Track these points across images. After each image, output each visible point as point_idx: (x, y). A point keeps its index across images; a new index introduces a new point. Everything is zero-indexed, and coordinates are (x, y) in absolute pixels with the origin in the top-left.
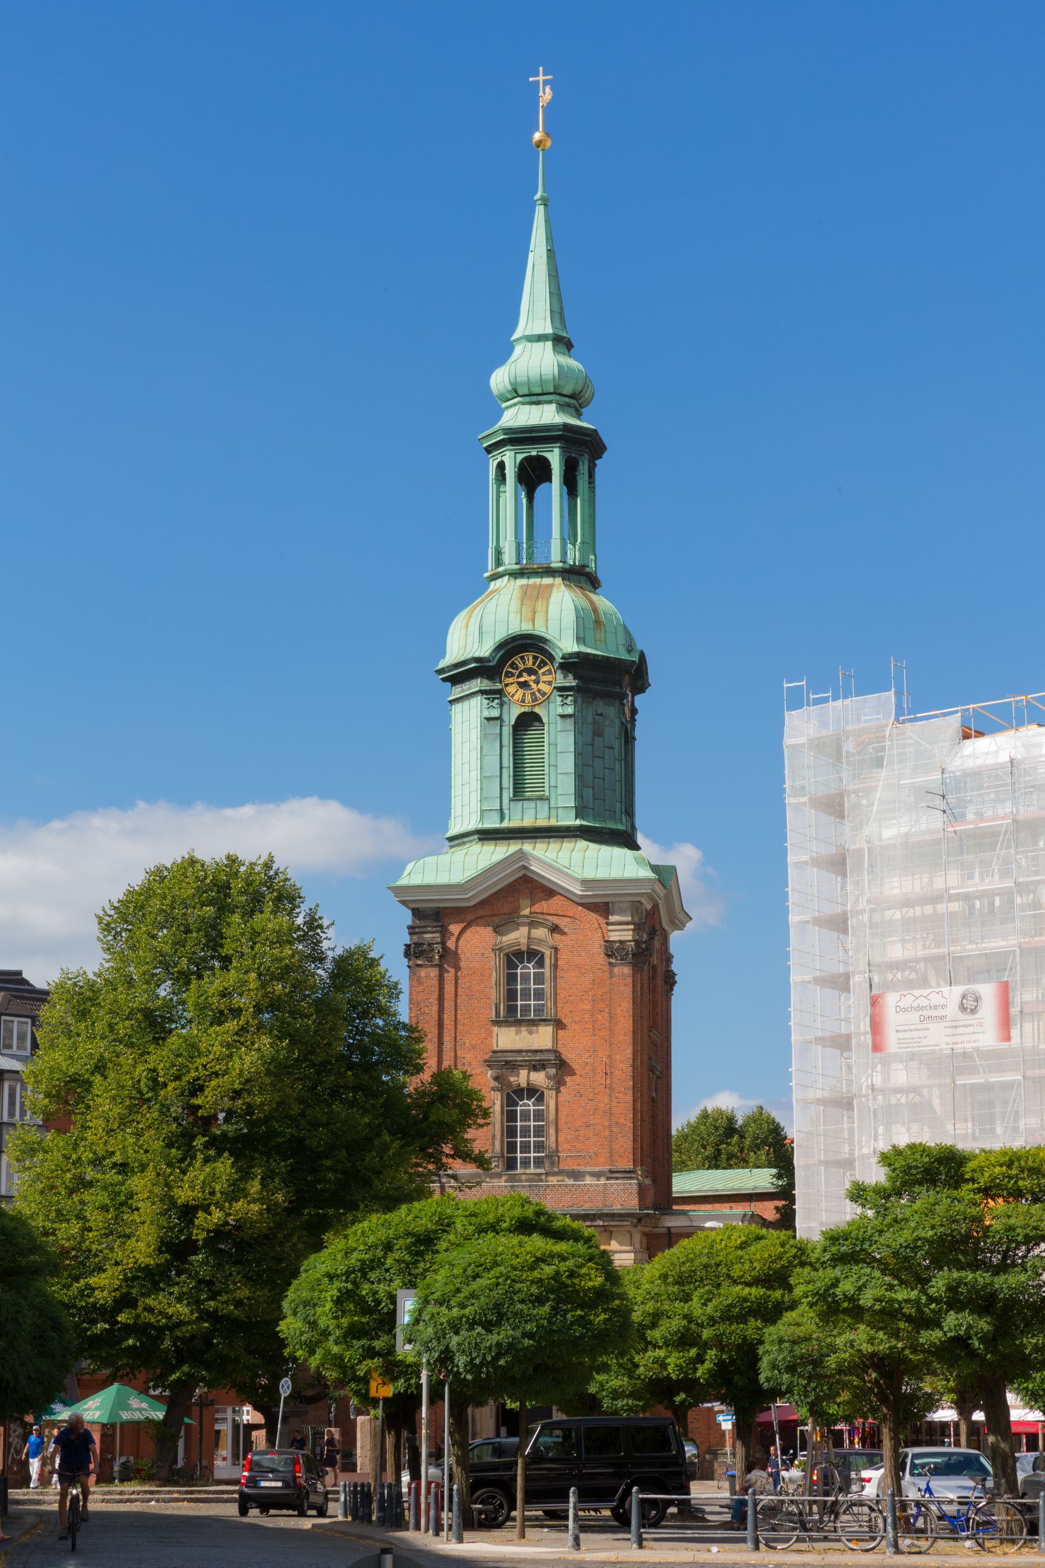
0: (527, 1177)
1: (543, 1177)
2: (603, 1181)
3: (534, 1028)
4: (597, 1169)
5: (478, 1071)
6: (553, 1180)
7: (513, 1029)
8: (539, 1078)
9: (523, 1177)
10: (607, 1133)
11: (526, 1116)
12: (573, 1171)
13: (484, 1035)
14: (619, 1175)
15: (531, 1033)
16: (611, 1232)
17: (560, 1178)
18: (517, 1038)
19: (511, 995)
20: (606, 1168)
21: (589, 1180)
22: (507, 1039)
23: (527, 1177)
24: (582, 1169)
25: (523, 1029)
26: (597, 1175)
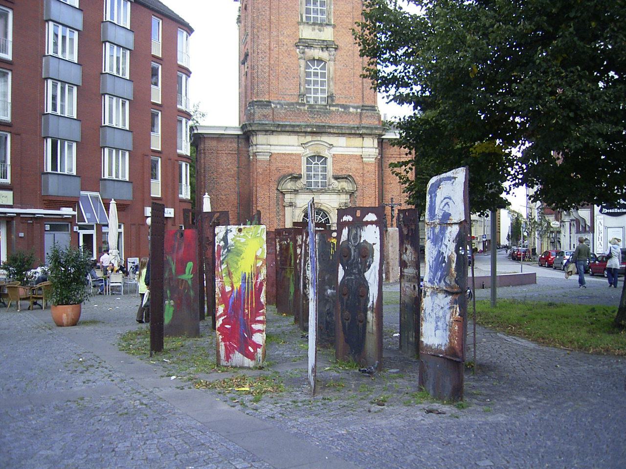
0: (319, 107)
1: (328, 107)
2: (359, 110)
3: (322, 28)
4: (356, 105)
5: (292, 48)
6: (333, 109)
7: (311, 27)
8: (325, 55)
9: (317, 107)
10: (361, 86)
11: (316, 74)
12: (343, 105)
13: (295, 30)
14: (368, 108)
15: (320, 31)
16: (363, 138)
17: (337, 108)
18: (313, 33)
19: (308, 11)
20: (361, 104)
21: (351, 110)
22: (307, 33)
23: (319, 107)
24: (348, 104)
25: (317, 27)
26: (357, 108)
